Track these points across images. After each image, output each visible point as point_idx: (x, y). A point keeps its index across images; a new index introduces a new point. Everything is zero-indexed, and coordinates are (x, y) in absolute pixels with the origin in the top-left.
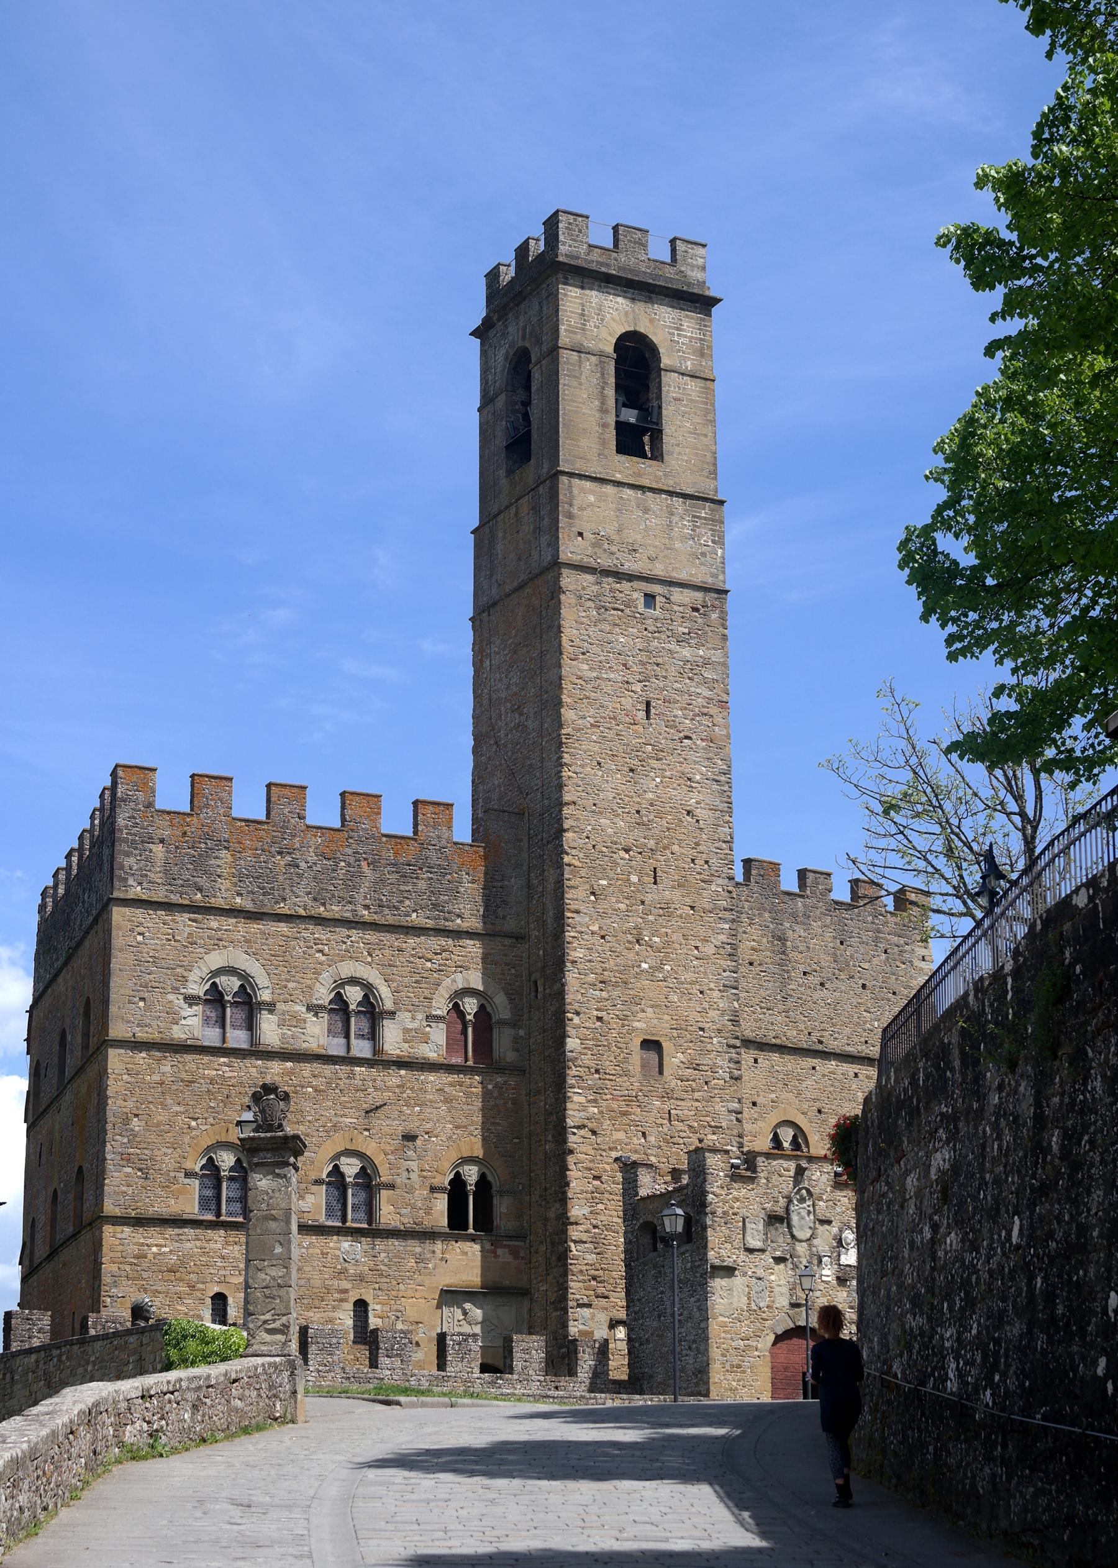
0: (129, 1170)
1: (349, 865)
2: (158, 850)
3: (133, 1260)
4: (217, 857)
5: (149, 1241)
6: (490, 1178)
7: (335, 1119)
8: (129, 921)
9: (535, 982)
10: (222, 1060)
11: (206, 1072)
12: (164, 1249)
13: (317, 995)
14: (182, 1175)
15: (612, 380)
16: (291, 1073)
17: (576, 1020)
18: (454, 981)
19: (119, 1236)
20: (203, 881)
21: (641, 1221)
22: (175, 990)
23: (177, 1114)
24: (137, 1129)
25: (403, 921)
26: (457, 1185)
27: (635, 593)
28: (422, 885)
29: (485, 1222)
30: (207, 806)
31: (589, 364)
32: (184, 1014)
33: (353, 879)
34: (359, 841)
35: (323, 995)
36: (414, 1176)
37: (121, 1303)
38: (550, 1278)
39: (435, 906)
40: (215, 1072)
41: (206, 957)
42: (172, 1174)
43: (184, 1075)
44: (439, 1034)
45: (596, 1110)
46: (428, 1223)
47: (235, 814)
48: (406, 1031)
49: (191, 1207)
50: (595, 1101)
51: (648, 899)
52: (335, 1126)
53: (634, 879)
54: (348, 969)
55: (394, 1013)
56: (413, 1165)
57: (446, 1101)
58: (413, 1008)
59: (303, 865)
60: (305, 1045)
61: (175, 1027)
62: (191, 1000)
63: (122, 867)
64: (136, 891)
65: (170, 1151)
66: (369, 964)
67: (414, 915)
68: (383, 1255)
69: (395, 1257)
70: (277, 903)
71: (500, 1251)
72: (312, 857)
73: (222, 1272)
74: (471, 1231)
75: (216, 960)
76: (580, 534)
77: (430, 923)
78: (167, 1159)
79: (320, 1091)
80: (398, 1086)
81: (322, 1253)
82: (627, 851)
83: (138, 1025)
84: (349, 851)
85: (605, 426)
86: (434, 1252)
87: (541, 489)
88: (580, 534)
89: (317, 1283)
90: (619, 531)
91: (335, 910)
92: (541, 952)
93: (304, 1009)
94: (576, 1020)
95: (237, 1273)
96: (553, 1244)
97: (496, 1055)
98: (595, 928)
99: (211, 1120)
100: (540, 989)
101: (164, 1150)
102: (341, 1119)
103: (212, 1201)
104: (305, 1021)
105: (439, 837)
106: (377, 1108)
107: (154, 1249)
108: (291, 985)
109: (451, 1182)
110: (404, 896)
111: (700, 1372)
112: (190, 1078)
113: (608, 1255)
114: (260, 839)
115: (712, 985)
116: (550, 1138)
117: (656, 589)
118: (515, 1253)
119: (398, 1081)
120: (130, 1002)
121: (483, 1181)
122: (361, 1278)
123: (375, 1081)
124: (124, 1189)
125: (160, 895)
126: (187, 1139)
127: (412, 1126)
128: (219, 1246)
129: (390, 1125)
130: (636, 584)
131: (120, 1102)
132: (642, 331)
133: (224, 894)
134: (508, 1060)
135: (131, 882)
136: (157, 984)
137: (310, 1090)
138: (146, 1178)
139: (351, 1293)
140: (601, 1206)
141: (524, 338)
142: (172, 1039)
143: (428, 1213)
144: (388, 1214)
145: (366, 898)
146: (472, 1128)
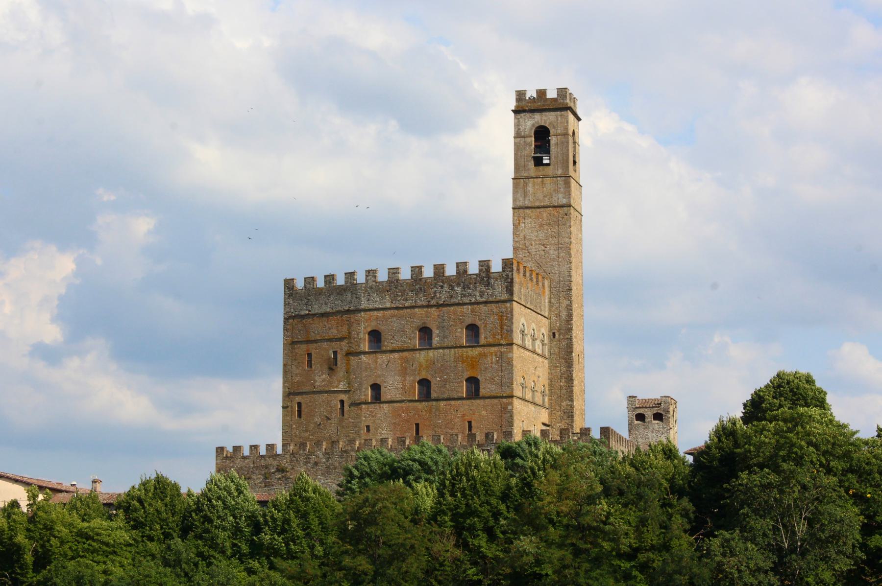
9: (554, 334)
38: (563, 422)
96: (564, 413)
100: (557, 335)
116: (563, 381)
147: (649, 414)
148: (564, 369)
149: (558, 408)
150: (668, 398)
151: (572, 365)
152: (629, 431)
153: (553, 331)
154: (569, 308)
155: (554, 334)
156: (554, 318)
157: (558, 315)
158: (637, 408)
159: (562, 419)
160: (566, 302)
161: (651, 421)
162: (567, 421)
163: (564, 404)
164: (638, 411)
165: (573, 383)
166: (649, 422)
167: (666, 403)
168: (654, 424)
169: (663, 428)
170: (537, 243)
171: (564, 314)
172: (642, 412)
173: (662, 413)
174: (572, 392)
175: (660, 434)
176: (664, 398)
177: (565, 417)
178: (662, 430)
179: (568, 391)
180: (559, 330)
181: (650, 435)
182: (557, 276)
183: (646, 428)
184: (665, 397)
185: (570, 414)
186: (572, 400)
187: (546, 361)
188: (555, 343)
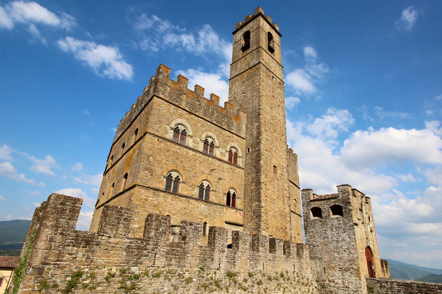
0: (146, 172)
1: (212, 110)
2: (169, 89)
3: (144, 201)
4: (182, 96)
5: (149, 195)
6: (236, 194)
7: (204, 171)
8: (158, 103)
9: (248, 149)
10: (177, 147)
11: (173, 149)
12: (153, 199)
13: (202, 138)
14: (163, 177)
15: (267, 38)
16: (194, 155)
17: (263, 157)
18: (231, 144)
19: (140, 192)
20: (178, 100)
21: (312, 207)
22: (168, 125)
23: (163, 159)
24: (151, 160)
25: (222, 127)
26: (229, 194)
27: (272, 75)
28: (226, 120)
29: (234, 205)
30: (182, 83)
31: (264, 33)
32: (169, 131)
33: (213, 113)
34: (214, 105)
35: (203, 138)
36: (220, 190)
37: (137, 215)
38: (253, 222)
39: (228, 126)
40: (175, 150)
41: (177, 119)
42: (160, 176)
43: (167, 148)
44: (227, 155)
45: (266, 180)
46: (222, 203)
47: (188, 88)
48: (221, 153)
49: (163, 187)
50: (266, 177)
51: (274, 135)
52: (203, 172)
53: (272, 130)
54: (210, 134)
55: (219, 147)
56: (221, 186)
57: (228, 172)
58: (223, 148)
59: (202, 106)
60: (198, 149)
61: (166, 134)
62: (172, 128)
63: (158, 89)
64: (162, 96)
65: (160, 169)
66: (214, 134)
67: (224, 126)
68: (212, 210)
69: (215, 211)
70: (195, 112)
71: (237, 213)
72: (204, 105)
73: (169, 209)
74: (231, 206)
75: (179, 121)
76: (263, 60)
77: (228, 129)
78: (158, 171)
79: (201, 162)
80: (218, 166)
81: (197, 207)
82: (271, 124)
83: (157, 131)
84: (212, 107)
85: (266, 44)
86: (223, 211)
87: (254, 52)
88: (263, 60)
89: (195, 215)
90: (269, 63)
91: (208, 119)
92: (251, 142)
93: (199, 140)
94: (263, 157)
95: (174, 210)
96: (254, 213)
97: (238, 164)
98: (266, 137)
99: (173, 163)
100: (250, 150)
101: (158, 168)
102: (205, 171)
103: (168, 186)
104: (199, 143)
105: (230, 111)
106: (213, 170)
107: (151, 198)
108: (197, 133)
109: (228, 193)
110: (223, 121)
111: (352, 260)
112: (168, 150)
113: (268, 217)
114: (193, 96)
115: (284, 157)
117: (274, 76)
118: (240, 214)
119: (218, 164)
120: (155, 124)
121: (234, 195)
122: (206, 216)
123: (213, 163)
124: (144, 177)
125: (167, 99)
126: (165, 166)
127: (221, 176)
128: (170, 200)
129: (216, 175)
130: (271, 73)
131: (147, 151)
132: (271, 33)
133: (183, 105)
134: (241, 166)
135: (160, 93)
136: (163, 122)
137: (198, 161)
138: (152, 176)
139: (203, 220)
140: (267, 204)
141: (248, 29)
142: (165, 138)
143: (223, 200)
144: (212, 198)
145: (215, 119)
146: (233, 180)
147: (325, 207)
148: (254, 175)
149: (249, 209)
150: (346, 187)
151: (260, 170)
152: (306, 229)
153: (248, 147)
154: (259, 128)
155: (248, 149)
156: (248, 137)
157: (251, 135)
158: (311, 201)
159: (252, 219)
160: (258, 124)
161: (329, 215)
162: (256, 220)
163: (254, 205)
164: (313, 205)
165: (260, 186)
166: (326, 217)
167: (344, 193)
168: (332, 219)
169: (345, 224)
170: (241, 93)
171: (255, 133)
172: (317, 206)
173: (340, 204)
174: (260, 193)
175: (341, 231)
176: (342, 187)
177: (255, 217)
178: (343, 226)
179: (257, 193)
180: (251, 146)
181: (329, 233)
182: (251, 109)
183: (324, 224)
184: (342, 186)
185: (258, 214)
186: (259, 201)
187: (242, 171)
188: (249, 156)
